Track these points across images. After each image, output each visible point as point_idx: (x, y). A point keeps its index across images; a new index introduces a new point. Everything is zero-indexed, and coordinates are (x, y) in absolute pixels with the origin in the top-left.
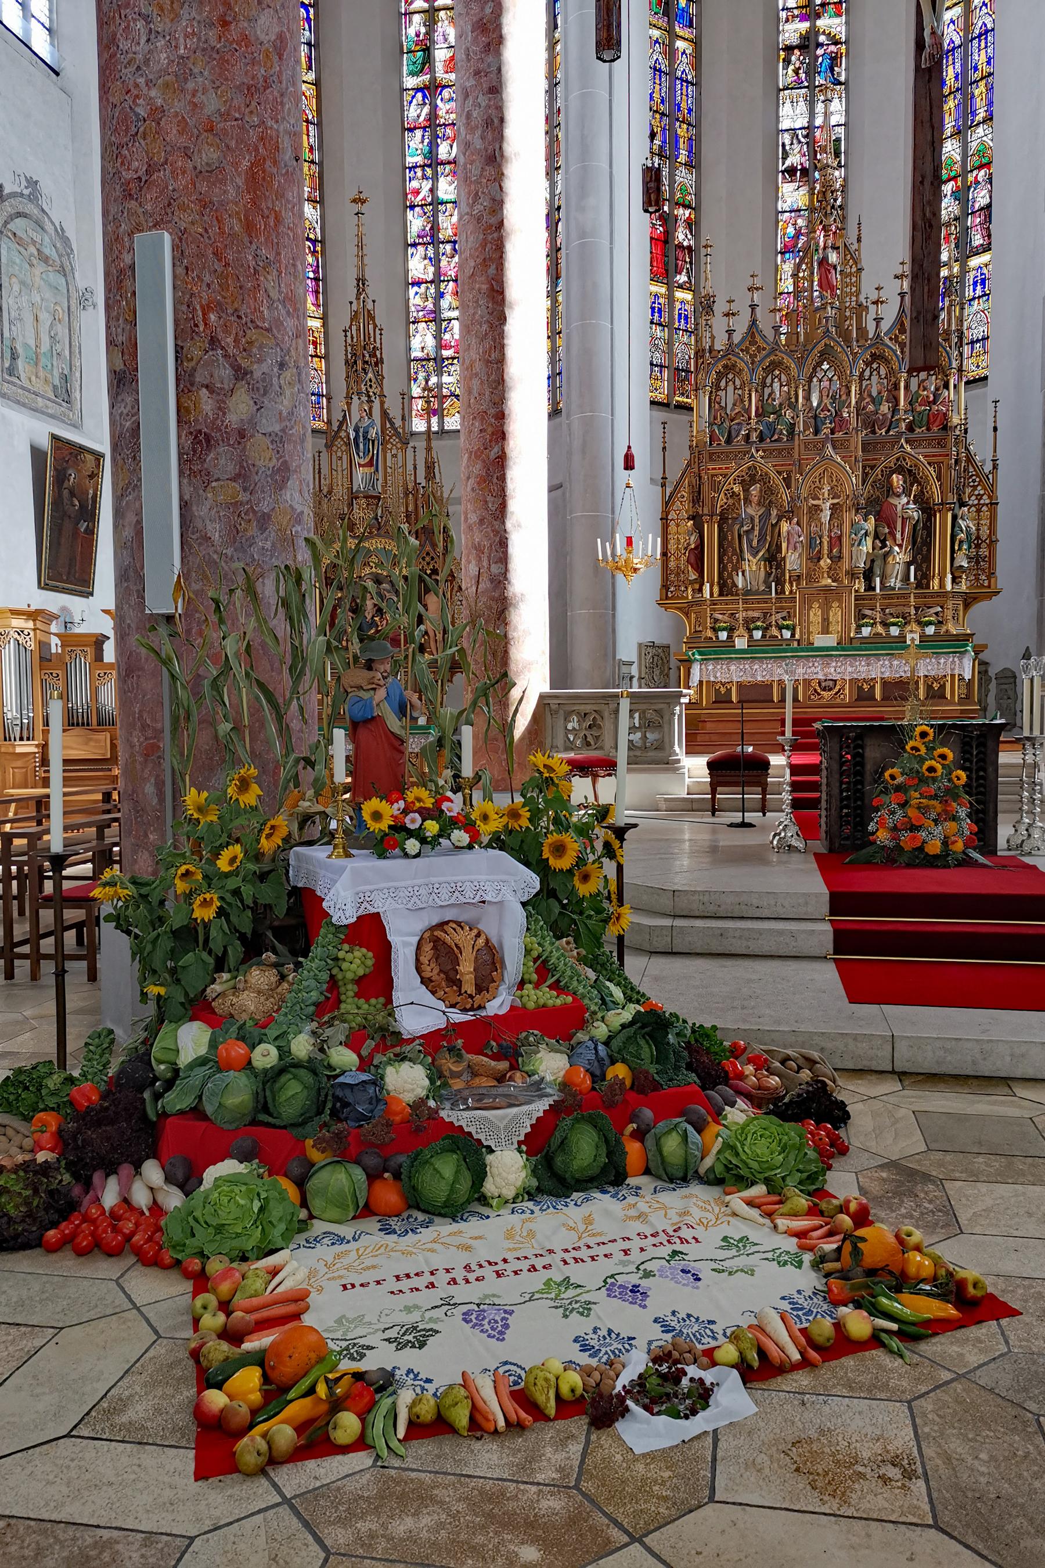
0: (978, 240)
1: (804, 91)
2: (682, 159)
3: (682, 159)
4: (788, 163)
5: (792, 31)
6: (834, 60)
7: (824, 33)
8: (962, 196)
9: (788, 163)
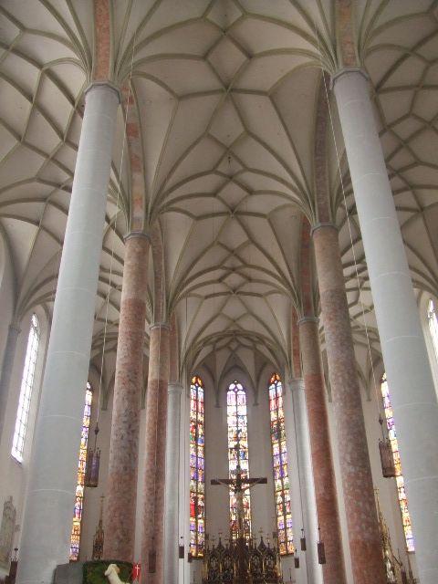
0: (288, 510)
2: (200, 480)
3: (200, 480)
5: (232, 444)
8: (283, 496)
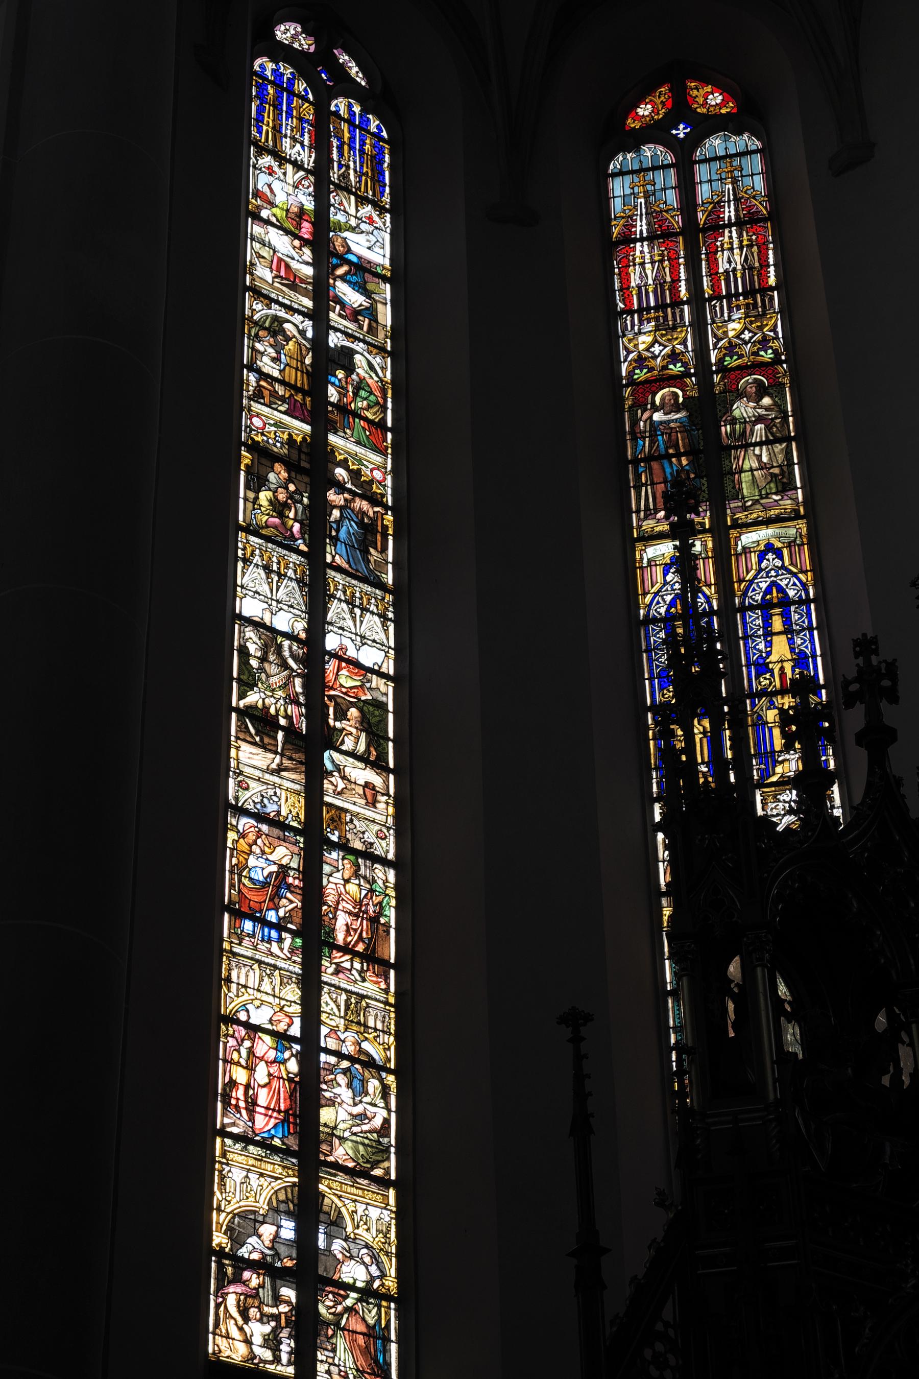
1: (294, 558)
4: (253, 698)
6: (369, 533)
7: (344, 464)
9: (253, 698)
